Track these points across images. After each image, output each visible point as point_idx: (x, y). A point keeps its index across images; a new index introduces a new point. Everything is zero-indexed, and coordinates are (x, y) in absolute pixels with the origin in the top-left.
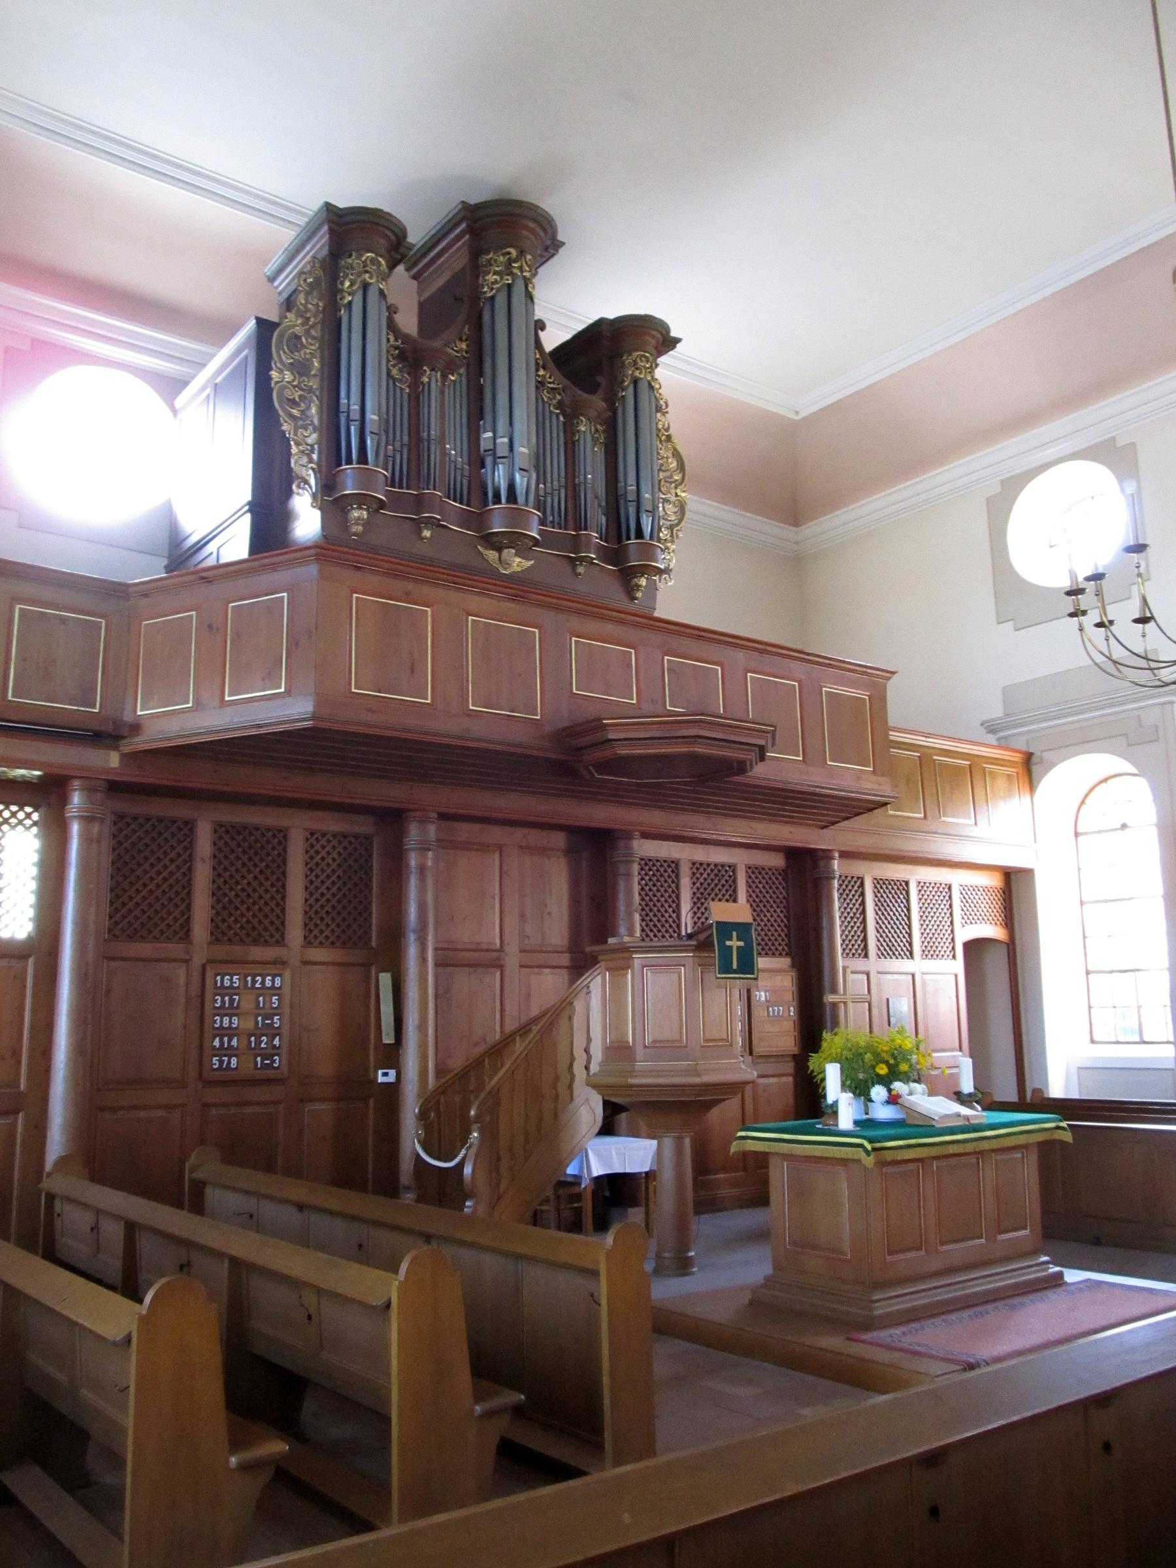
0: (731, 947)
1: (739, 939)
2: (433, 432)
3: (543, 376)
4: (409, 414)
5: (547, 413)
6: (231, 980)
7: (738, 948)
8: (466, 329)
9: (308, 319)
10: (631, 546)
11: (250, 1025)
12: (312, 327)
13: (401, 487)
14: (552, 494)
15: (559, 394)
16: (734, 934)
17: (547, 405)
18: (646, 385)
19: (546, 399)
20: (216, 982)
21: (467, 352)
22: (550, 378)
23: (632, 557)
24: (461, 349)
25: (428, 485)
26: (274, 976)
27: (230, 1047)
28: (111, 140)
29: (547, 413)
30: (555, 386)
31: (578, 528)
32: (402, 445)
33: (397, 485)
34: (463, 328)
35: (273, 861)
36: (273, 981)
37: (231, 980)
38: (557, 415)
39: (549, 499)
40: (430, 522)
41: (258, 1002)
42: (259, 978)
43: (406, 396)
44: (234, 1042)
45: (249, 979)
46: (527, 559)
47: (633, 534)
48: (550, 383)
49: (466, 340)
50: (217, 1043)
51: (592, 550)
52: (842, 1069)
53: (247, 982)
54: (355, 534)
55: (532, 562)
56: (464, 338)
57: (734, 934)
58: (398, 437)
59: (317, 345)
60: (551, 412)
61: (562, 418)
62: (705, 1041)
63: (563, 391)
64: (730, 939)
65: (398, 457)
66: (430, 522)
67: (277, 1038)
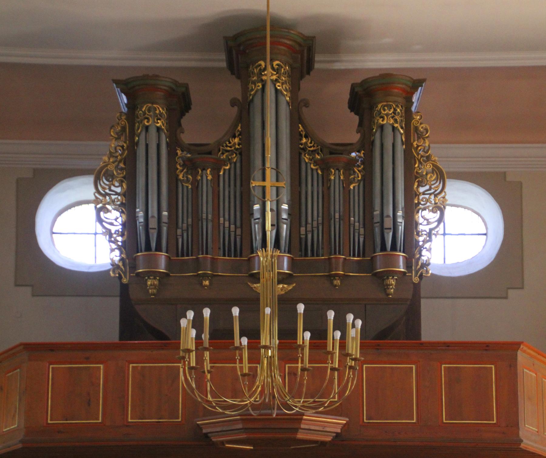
3: (306, 143)
4: (192, 204)
5: (309, 172)
8: (239, 128)
9: (117, 157)
10: (378, 257)
12: (120, 162)
13: (188, 256)
14: (312, 232)
15: (318, 154)
17: (309, 164)
18: (390, 129)
19: (307, 161)
21: (239, 145)
22: (311, 143)
23: (378, 266)
24: (235, 144)
25: (199, 252)
29: (309, 172)
30: (315, 148)
31: (331, 254)
32: (188, 225)
34: (237, 126)
38: (317, 170)
39: (310, 236)
40: (205, 276)
43: (190, 191)
46: (289, 284)
47: (378, 248)
48: (311, 147)
49: (239, 135)
51: (341, 269)
54: (152, 295)
55: (294, 285)
56: (237, 135)
58: (185, 222)
59: (124, 173)
60: (312, 169)
61: (320, 172)
63: (321, 151)
65: (185, 235)
66: (205, 276)
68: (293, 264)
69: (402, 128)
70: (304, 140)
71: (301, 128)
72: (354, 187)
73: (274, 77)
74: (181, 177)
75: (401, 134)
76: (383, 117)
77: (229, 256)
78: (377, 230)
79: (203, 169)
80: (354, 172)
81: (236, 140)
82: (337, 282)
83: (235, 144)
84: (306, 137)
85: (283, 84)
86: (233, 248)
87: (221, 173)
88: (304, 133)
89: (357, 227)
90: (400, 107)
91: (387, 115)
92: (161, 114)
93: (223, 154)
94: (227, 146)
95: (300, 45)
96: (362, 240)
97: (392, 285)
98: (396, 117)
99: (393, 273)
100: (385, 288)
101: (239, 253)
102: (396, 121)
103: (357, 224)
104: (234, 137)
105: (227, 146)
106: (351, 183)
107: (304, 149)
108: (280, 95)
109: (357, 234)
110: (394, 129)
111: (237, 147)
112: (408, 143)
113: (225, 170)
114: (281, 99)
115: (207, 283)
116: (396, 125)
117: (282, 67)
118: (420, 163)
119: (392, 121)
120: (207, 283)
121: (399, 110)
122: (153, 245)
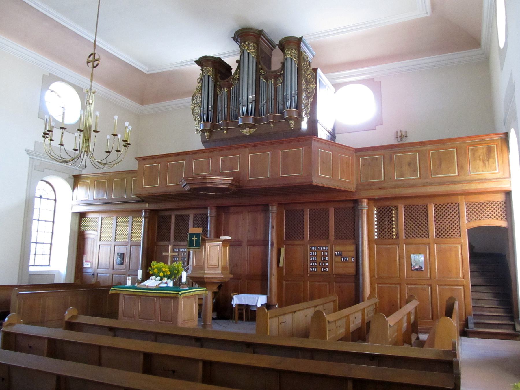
0: (193, 240)
1: (196, 238)
2: (225, 105)
6: (314, 248)
7: (196, 240)
11: (319, 260)
16: (195, 236)
20: (310, 248)
26: (325, 247)
27: (315, 265)
28: (185, 62)
29: (263, 82)
33: (231, 120)
35: (185, 222)
36: (325, 248)
37: (314, 248)
41: (322, 254)
42: (321, 247)
44: (316, 264)
45: (319, 248)
50: (311, 264)
52: (142, 271)
53: (318, 248)
57: (195, 236)
60: (264, 81)
62: (209, 265)
64: (194, 238)
67: (327, 263)
68: (255, 120)
69: (295, 58)
70: (261, 71)
71: (260, 66)
72: (279, 86)
73: (246, 48)
74: (218, 93)
75: (295, 61)
76: (286, 55)
77: (232, 120)
78: (285, 101)
79: (224, 88)
80: (279, 80)
81: (237, 75)
82: (272, 125)
83: (237, 77)
84: (262, 69)
85: (250, 50)
86: (233, 116)
87: (231, 88)
88: (261, 68)
89: (280, 102)
90: (294, 50)
91: (288, 54)
92: (209, 70)
93: (232, 81)
94: (234, 78)
95: (257, 34)
96: (282, 107)
97: (292, 123)
98: (292, 54)
99: (291, 118)
100: (289, 125)
101: (235, 119)
102: (292, 56)
103: (280, 101)
104: (237, 74)
105: (234, 78)
106: (277, 84)
107: (261, 74)
108: (249, 54)
109: (280, 105)
110: (291, 59)
111: (238, 78)
112: (299, 64)
113: (233, 88)
114: (250, 55)
115: (225, 132)
116: (291, 57)
117: (250, 44)
118: (305, 71)
119: (290, 56)
120: (225, 132)
121: (293, 51)
122: (205, 119)
